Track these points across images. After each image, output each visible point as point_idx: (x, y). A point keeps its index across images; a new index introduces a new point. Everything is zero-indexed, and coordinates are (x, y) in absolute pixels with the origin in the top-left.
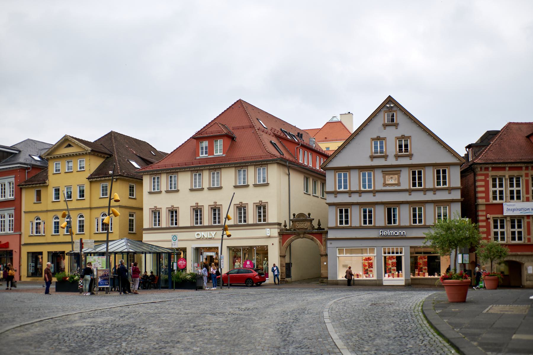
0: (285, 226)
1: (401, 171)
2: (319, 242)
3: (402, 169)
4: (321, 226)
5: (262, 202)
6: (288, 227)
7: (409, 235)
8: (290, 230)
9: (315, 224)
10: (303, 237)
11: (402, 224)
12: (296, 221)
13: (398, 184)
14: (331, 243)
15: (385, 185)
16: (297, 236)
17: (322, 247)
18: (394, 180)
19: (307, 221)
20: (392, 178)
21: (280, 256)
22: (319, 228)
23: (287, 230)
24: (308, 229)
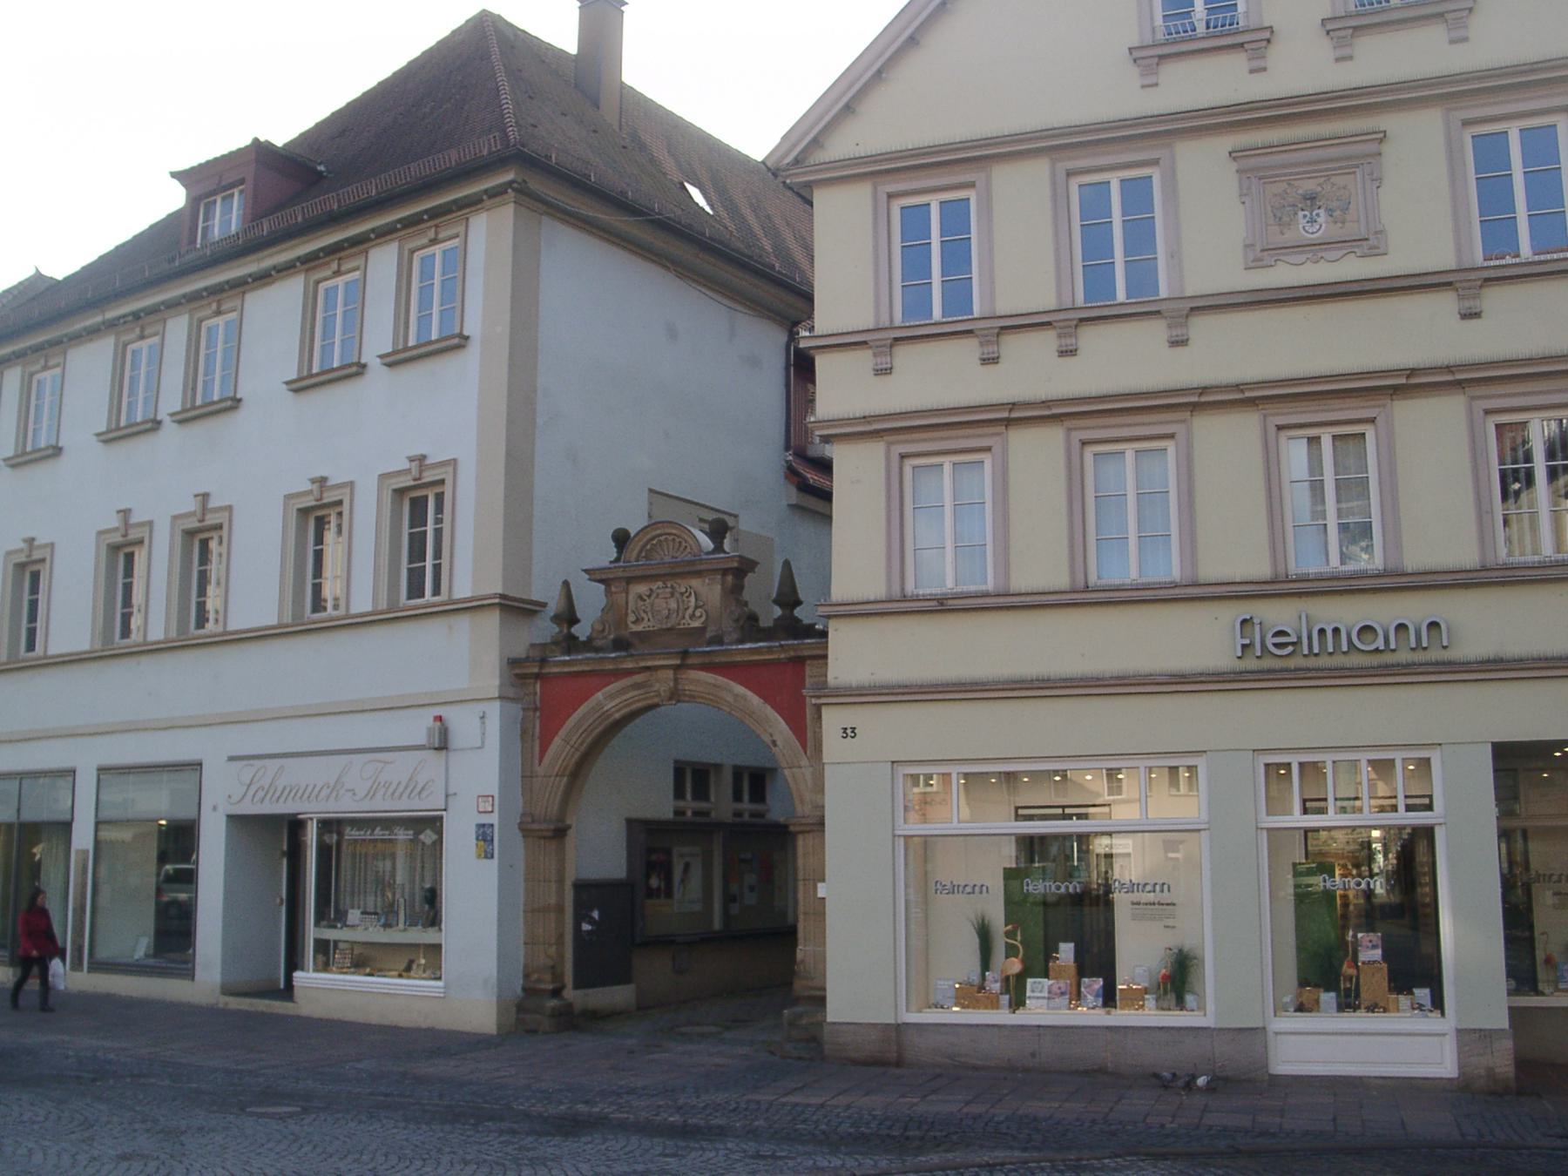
0: (568, 617)
1: (1383, 137)
2: (782, 725)
3: (1389, 122)
4: (797, 612)
5: (428, 462)
6: (582, 631)
7: (1471, 647)
8: (588, 645)
9: (760, 594)
10: (676, 695)
11: (1416, 558)
12: (630, 580)
13: (1368, 243)
14: (849, 733)
15: (1262, 254)
16: (636, 686)
17: (804, 762)
18: (1330, 212)
19: (699, 574)
20: (1311, 199)
21: (526, 831)
22: (793, 628)
23: (570, 644)
24: (708, 635)
